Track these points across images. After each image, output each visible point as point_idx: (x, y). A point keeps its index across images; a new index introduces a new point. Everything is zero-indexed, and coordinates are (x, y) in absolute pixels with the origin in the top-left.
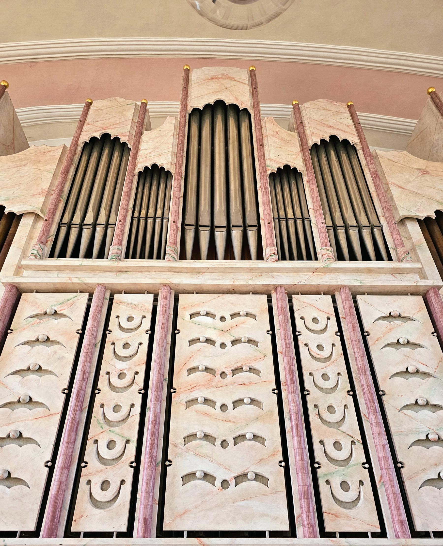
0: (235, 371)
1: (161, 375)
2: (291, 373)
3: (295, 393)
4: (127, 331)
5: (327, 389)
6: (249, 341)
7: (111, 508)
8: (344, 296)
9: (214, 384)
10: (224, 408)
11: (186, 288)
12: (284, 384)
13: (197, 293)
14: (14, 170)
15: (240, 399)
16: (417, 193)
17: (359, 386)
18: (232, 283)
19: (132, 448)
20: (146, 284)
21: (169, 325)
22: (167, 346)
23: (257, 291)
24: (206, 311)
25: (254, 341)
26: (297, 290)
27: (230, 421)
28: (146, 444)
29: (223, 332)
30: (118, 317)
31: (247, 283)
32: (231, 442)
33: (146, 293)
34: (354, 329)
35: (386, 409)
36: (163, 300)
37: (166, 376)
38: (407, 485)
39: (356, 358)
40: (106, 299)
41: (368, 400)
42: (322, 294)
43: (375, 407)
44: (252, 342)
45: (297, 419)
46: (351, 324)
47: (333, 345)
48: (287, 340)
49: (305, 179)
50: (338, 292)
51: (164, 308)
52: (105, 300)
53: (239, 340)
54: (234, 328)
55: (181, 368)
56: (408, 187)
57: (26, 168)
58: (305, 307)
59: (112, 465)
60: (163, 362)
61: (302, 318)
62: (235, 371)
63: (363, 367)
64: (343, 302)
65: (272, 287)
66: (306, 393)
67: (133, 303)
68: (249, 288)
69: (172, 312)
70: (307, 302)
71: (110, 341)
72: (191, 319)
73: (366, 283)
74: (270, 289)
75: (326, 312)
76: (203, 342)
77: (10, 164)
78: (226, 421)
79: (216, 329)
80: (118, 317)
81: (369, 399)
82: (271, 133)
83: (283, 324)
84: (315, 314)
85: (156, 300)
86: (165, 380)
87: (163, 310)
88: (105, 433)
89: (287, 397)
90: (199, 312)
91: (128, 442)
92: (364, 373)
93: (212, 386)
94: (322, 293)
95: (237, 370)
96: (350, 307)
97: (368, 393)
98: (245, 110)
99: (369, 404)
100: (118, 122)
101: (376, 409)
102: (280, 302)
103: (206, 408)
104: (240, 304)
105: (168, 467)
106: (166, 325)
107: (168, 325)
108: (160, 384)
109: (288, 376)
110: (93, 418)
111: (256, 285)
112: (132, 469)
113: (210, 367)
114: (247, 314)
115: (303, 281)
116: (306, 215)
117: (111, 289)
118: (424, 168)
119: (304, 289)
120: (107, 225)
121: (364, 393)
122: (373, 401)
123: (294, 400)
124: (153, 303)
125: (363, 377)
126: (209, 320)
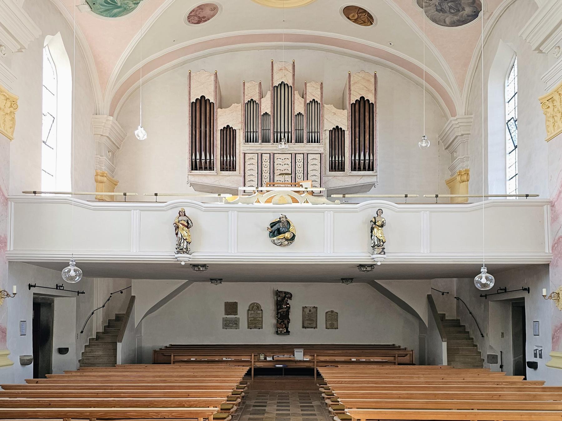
6: (287, 164)
14: (231, 114)
16: (330, 122)
49: (304, 116)
56: (329, 120)
57: (234, 113)
77: (229, 112)
98: (290, 86)
116: (303, 129)
118: (335, 112)
126: (280, 159)
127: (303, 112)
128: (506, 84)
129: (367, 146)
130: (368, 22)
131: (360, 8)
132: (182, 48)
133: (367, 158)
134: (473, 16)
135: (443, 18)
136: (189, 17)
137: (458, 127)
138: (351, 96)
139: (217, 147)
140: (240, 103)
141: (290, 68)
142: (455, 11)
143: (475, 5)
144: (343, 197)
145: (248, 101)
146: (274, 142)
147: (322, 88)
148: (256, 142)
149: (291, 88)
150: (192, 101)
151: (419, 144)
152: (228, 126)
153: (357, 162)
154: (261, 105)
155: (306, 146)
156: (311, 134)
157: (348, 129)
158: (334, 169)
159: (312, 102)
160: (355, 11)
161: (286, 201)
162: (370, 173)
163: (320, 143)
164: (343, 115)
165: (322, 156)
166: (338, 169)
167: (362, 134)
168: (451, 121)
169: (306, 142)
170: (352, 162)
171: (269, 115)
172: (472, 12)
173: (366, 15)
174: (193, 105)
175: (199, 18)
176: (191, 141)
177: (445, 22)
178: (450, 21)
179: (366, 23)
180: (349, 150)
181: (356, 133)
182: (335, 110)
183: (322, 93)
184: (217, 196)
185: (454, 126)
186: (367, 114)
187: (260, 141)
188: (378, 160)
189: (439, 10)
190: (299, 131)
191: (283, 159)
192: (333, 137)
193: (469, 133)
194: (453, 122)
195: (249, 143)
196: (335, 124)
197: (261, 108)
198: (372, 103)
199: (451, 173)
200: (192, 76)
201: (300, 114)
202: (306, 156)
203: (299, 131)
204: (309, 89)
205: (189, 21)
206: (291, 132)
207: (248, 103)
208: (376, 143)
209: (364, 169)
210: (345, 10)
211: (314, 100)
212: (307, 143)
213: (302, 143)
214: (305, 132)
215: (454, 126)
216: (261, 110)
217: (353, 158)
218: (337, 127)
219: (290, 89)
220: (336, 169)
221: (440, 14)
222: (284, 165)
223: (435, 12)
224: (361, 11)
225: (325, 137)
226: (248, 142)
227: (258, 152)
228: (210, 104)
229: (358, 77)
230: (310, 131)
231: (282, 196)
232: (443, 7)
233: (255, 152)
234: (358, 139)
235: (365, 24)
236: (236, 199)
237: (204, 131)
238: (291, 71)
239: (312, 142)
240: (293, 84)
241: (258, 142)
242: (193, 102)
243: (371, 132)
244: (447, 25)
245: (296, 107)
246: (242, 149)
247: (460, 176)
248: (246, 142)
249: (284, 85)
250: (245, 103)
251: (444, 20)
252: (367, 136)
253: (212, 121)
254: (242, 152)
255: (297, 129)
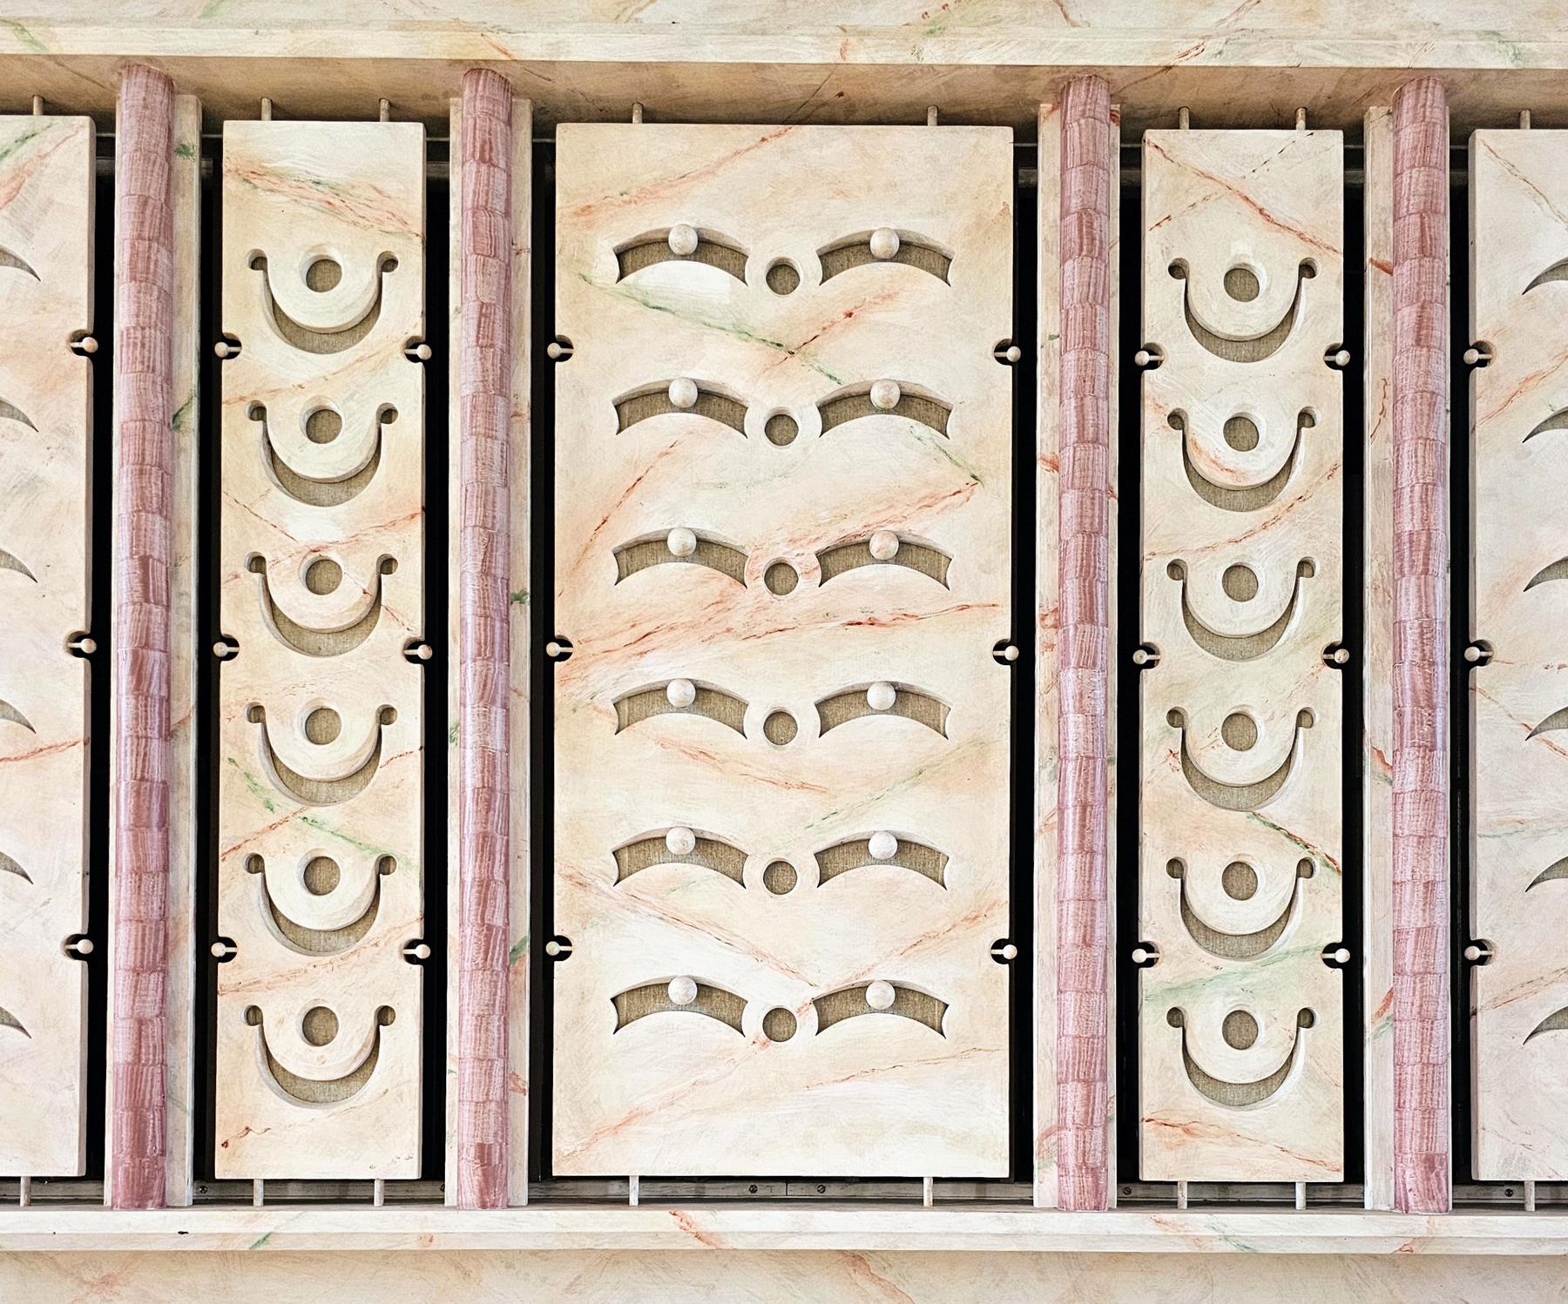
0: (831, 560)
1: (495, 581)
2: (1088, 574)
3: (1094, 664)
4: (317, 340)
5: (1239, 638)
7: (350, 1102)
8: (1409, 135)
9: (737, 620)
10: (779, 727)
11: (589, 86)
12: (1050, 621)
13: (649, 117)
15: (851, 690)
17: (1385, 624)
18: (832, 57)
19: (406, 891)
20: (376, 60)
21: (515, 313)
22: (516, 427)
23: (962, 104)
24: (698, 231)
25: (928, 401)
26: (1180, 96)
27: (803, 786)
28: (462, 882)
29: (783, 354)
30: (258, 262)
31: (912, 60)
32: (808, 870)
33: (383, 114)
34: (1421, 338)
35: (1479, 727)
36: (472, 167)
37: (523, 580)
38: (1485, 1028)
39: (1397, 492)
40: (184, 150)
41: (1409, 693)
42: (1301, 123)
43: (1432, 725)
44: (921, 408)
45: (1085, 785)
46: (1415, 308)
47: (1305, 418)
48: (1088, 401)
50: (1384, 110)
51: (484, 218)
52: (179, 160)
53: (859, 396)
54: (837, 329)
55: (585, 540)
58: (1200, 206)
59: (334, 950)
60: (498, 514)
61: (1177, 270)
62: (831, 560)
63: (1424, 538)
64: (1396, 175)
65: (1044, 82)
66: (1140, 657)
67: (325, 175)
68: (922, 89)
69: (525, 238)
70: (1215, 173)
71: (242, 399)
72: (621, 276)
73: (1546, 58)
74: (1033, 89)
75: (1300, 235)
76: (684, 410)
78: (787, 786)
79: (745, 334)
80: (258, 262)
81: (1414, 690)
83: (1080, 313)
84: (1251, 244)
85: (437, 151)
86: (519, 598)
87: (475, 226)
88: (285, 829)
89: (1056, 681)
90: (661, 236)
91: (385, 865)
92: (1421, 568)
93: (728, 630)
94: (1301, 113)
95: (842, 552)
96: (1427, 211)
97: (1417, 660)
99: (1408, 709)
101: (1434, 734)
102: (1075, 179)
103: (703, 728)
104: (870, 189)
105: (556, 963)
106: (500, 314)
107: (508, 313)
108: (498, 624)
109: (1072, 586)
110: (224, 766)
111: (960, 67)
112: (418, 969)
113: (721, 539)
114: (908, 250)
115: (1213, 46)
117: (200, 91)
119: (1212, 95)
121: (1398, 660)
122: (1430, 698)
123: (1086, 701)
124: (427, 170)
125: (1410, 585)
126: (709, 279)
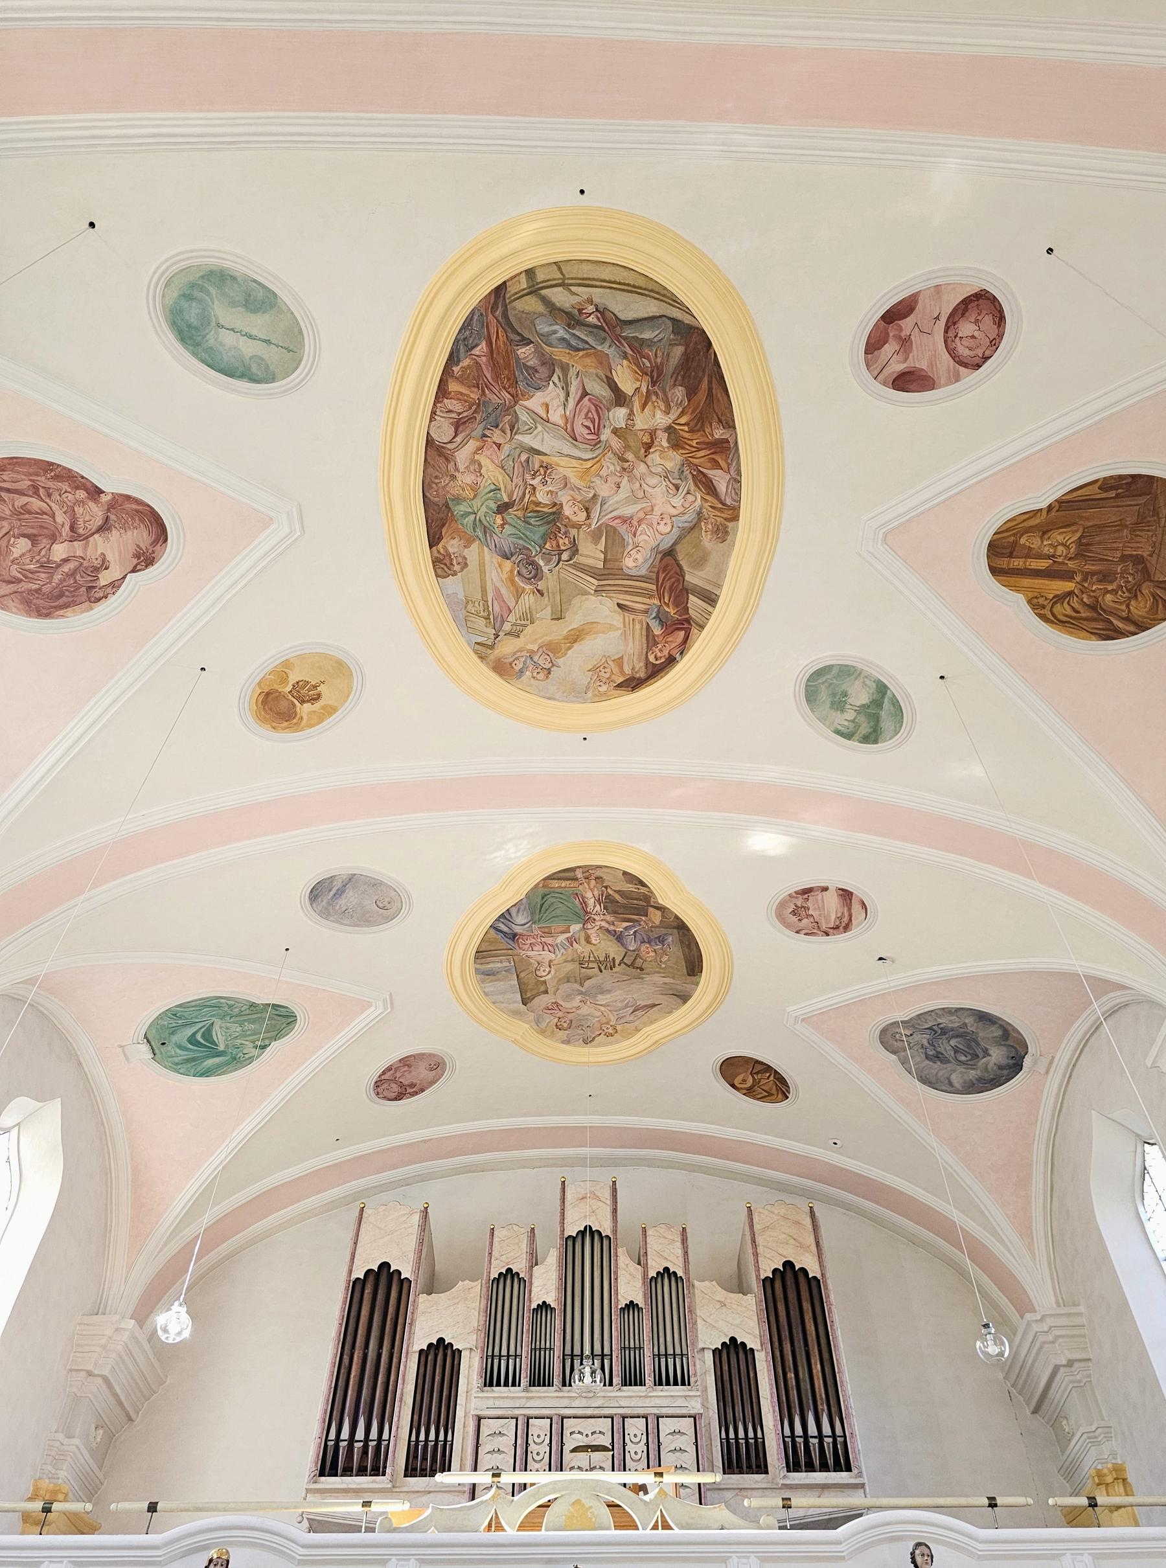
14: (452, 1308)
56: (709, 1320)
77: (448, 1302)
82: (624, 1266)
84: (635, 1432)
98: (607, 1236)
100: (516, 1256)
116: (642, 1346)
118: (723, 1300)
120: (516, 1356)
127: (639, 1300)
128: (1144, 1217)
129: (821, 1395)
130: (778, 1094)
131: (757, 1062)
132: (353, 1159)
133: (826, 1430)
134: (1011, 1068)
135: (946, 1076)
136: (377, 1084)
137: (1053, 1342)
138: (760, 1259)
139: (403, 1404)
140: (477, 1280)
141: (607, 1195)
142: (969, 1057)
143: (1010, 1042)
144: (784, 1507)
145: (501, 1274)
146: (564, 1385)
147: (684, 1240)
148: (514, 1385)
149: (608, 1241)
150: (354, 1276)
151: (978, 1347)
152: (441, 1340)
153: (800, 1443)
154: (531, 1284)
155: (651, 1394)
156: (663, 1360)
157: (762, 1346)
158: (737, 1467)
159: (662, 1275)
160: (748, 1069)
161: (594, 1519)
162: (842, 1477)
163: (689, 1385)
164: (744, 1309)
165: (700, 1424)
166: (749, 1467)
167: (802, 1359)
168: (1029, 1324)
169: (652, 1384)
170: (784, 1441)
171: (552, 1309)
172: (1008, 1057)
173: (772, 1078)
174: (357, 1287)
175: (401, 1085)
176: (333, 1386)
177: (951, 1084)
178: (961, 1081)
179: (772, 1095)
180: (773, 1407)
181: (786, 1356)
182: (721, 1294)
183: (686, 1253)
184: (359, 1508)
185: (1041, 1339)
186: (806, 1306)
187: (525, 1381)
188: (858, 1437)
189: (933, 1056)
190: (632, 1352)
191: (587, 1435)
192: (725, 1368)
193: (1088, 1357)
194: (1036, 1328)
195: (495, 1388)
196: (726, 1331)
197: (530, 1291)
198: (815, 1278)
199: (1071, 1486)
200: (366, 1215)
201: (631, 1305)
202: (653, 1422)
203: (632, 1352)
204: (654, 1244)
205: (378, 1094)
206: (611, 1355)
207: (498, 1280)
208: (845, 1383)
209: (824, 1467)
210: (723, 1067)
211: (666, 1269)
212: (655, 1385)
213: (641, 1385)
214: (647, 1353)
215: (1041, 1339)
216: (530, 1295)
217: (787, 1432)
218: (733, 1339)
219: (605, 1242)
220: (742, 1468)
221: (935, 1066)
222: (592, 1434)
223: (924, 1061)
224: (758, 1068)
225: (704, 1369)
226: (493, 1386)
227: (517, 1412)
228: (401, 1282)
229: (771, 1215)
230: (662, 1351)
231: (578, 1502)
232: (939, 1049)
233: (509, 1413)
234: (793, 1376)
235: (769, 1098)
236: (420, 1516)
237: (375, 1355)
238: (608, 1202)
239: (668, 1384)
240: (615, 1231)
241: (519, 1386)
242: (358, 1279)
243: (826, 1356)
244: (958, 1090)
245: (623, 1287)
246: (473, 1406)
247: (1103, 1488)
248: (485, 1386)
249: (592, 1233)
250: (492, 1278)
251: (949, 1079)
252: (816, 1365)
253: (399, 1328)
254: (472, 1413)
255: (625, 1348)
